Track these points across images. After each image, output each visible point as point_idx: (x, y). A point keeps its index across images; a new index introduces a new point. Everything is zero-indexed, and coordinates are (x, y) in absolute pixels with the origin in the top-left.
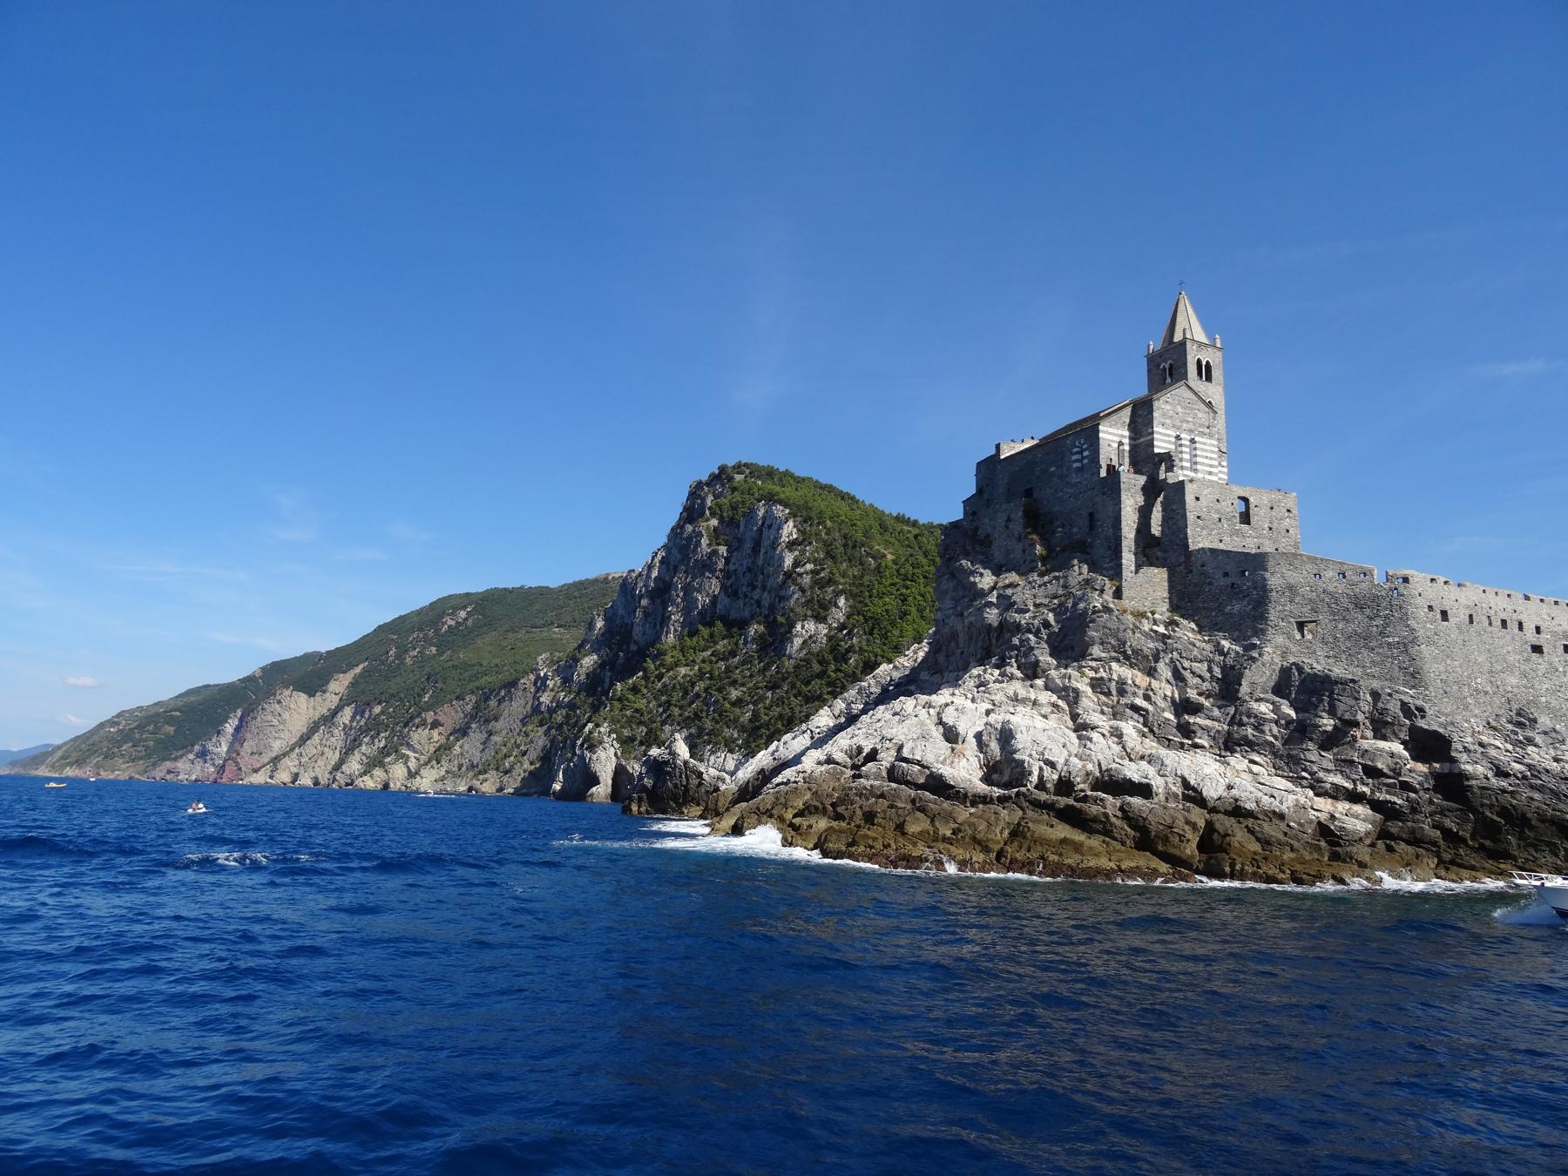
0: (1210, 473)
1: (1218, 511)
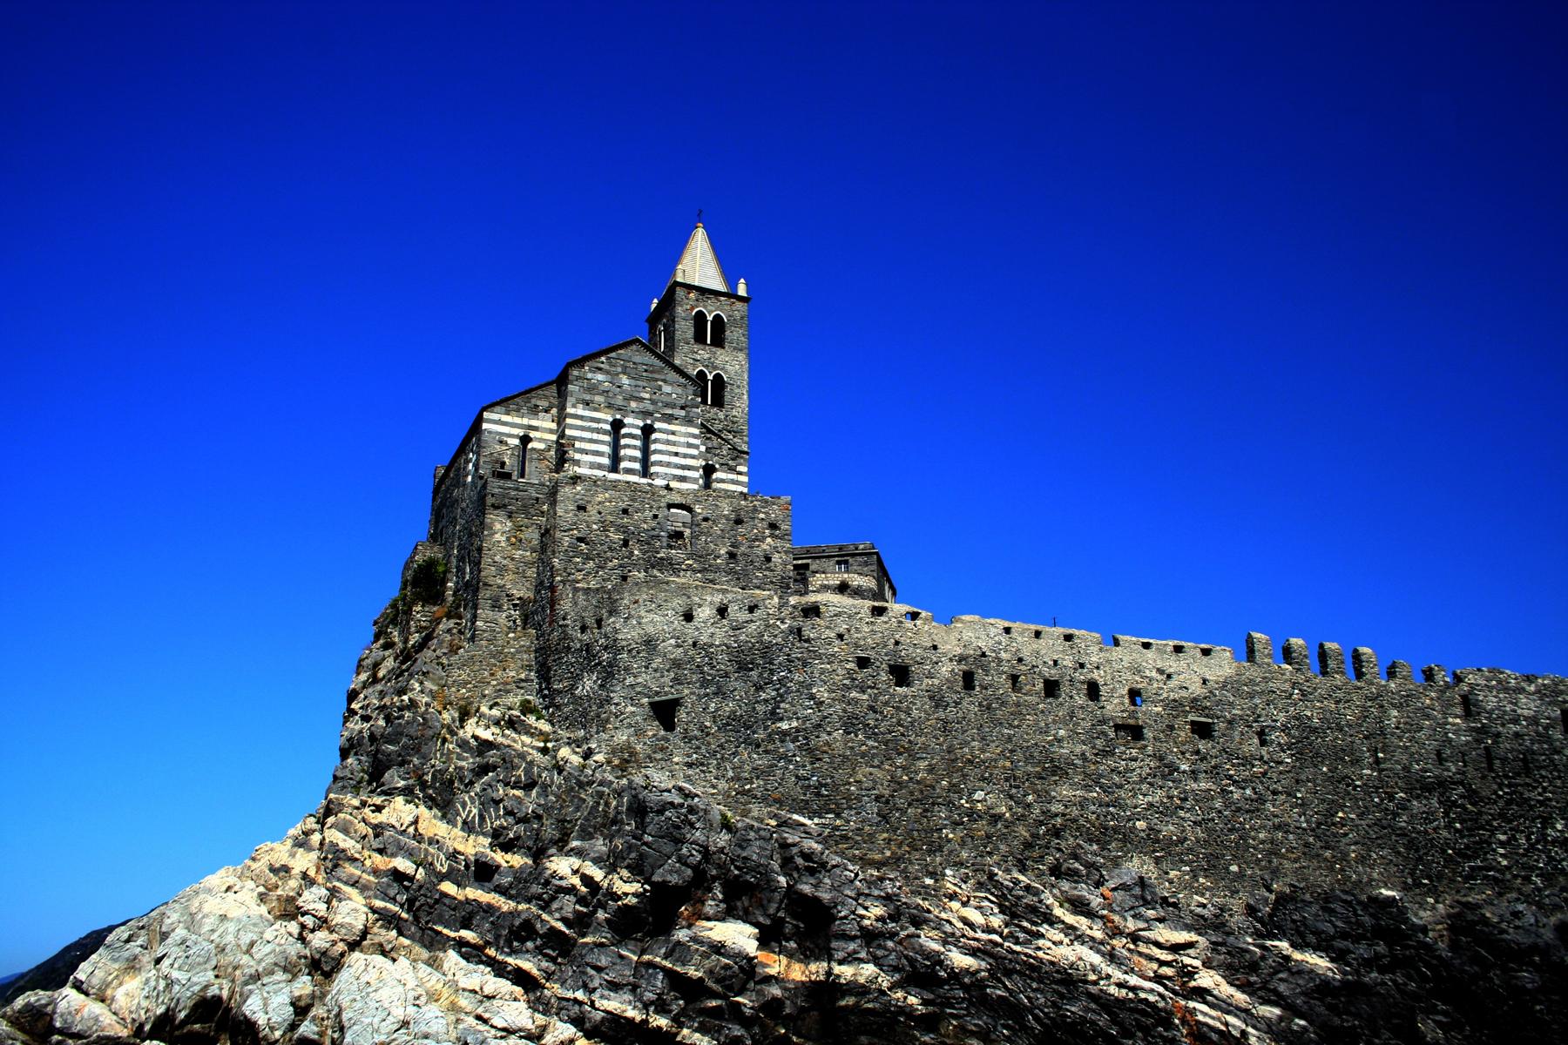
0: (683, 479)
1: (622, 529)
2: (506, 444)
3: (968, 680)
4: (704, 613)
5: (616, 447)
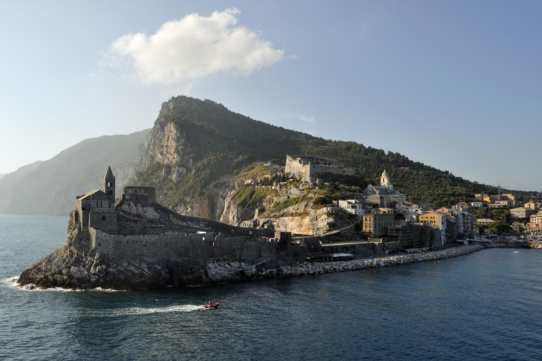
3: (127, 242)
4: (103, 235)
5: (97, 204)
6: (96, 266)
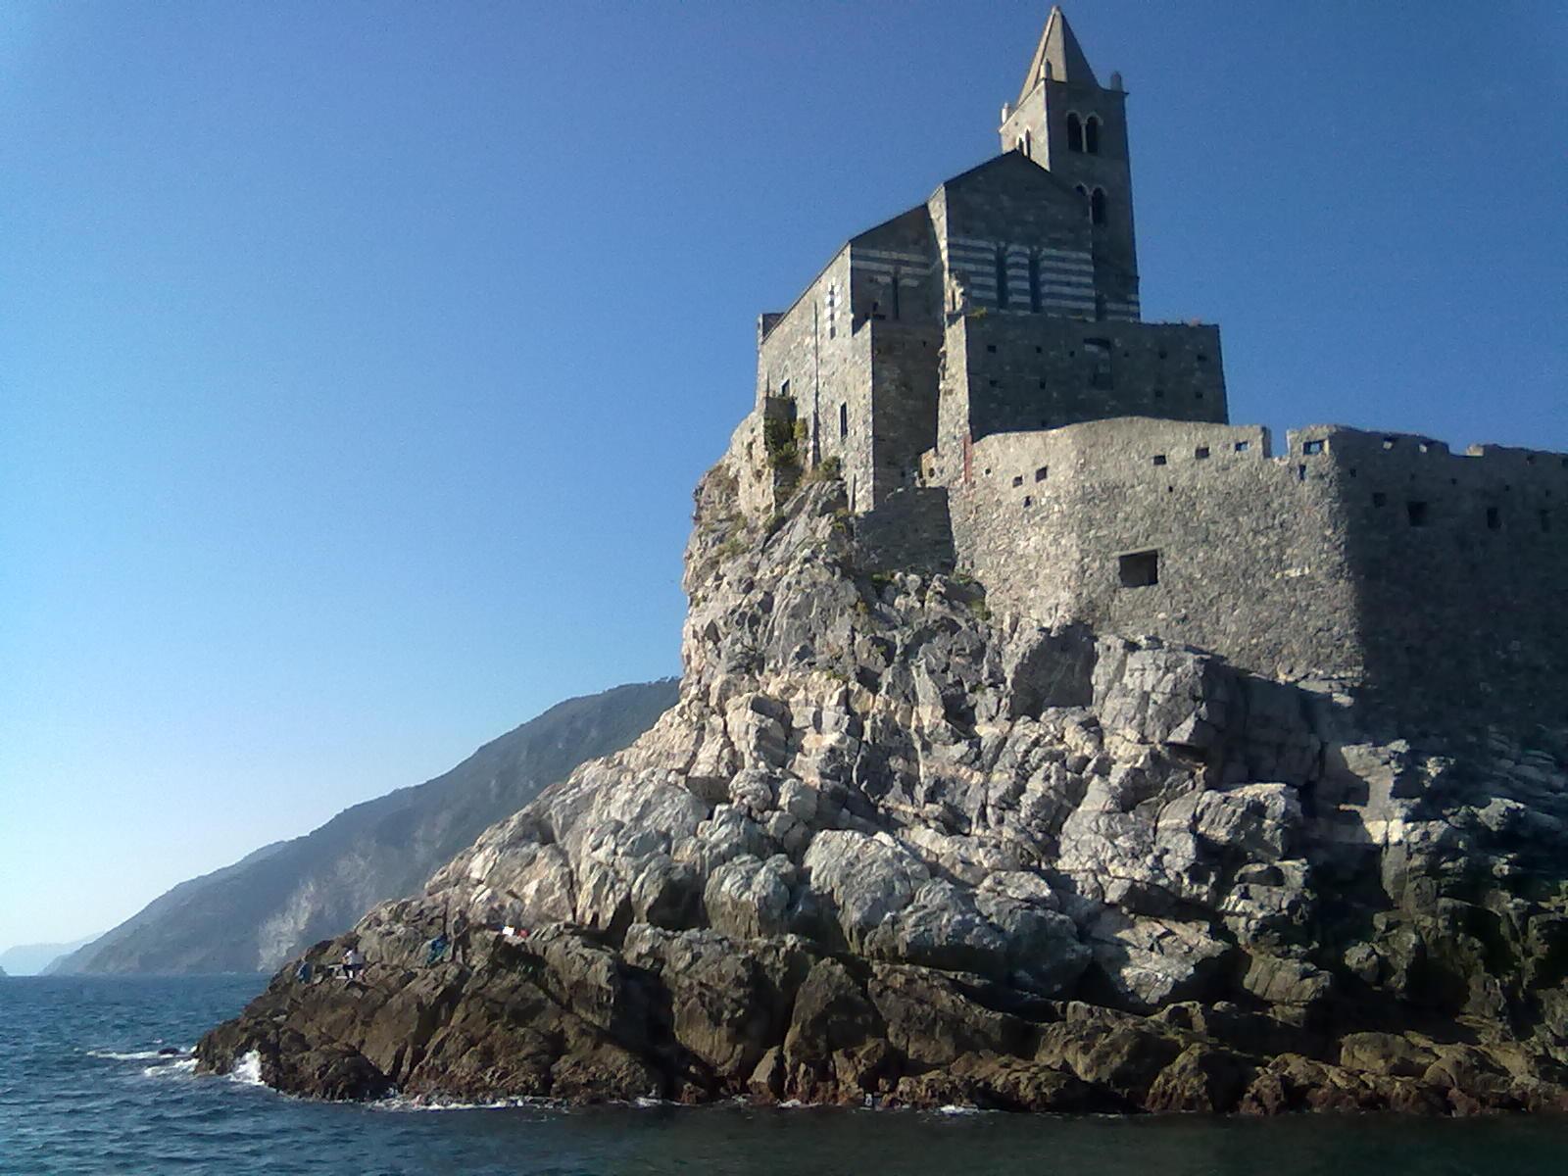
2: (876, 281)
3: (1492, 516)
5: (1002, 278)
6: (1135, 795)
